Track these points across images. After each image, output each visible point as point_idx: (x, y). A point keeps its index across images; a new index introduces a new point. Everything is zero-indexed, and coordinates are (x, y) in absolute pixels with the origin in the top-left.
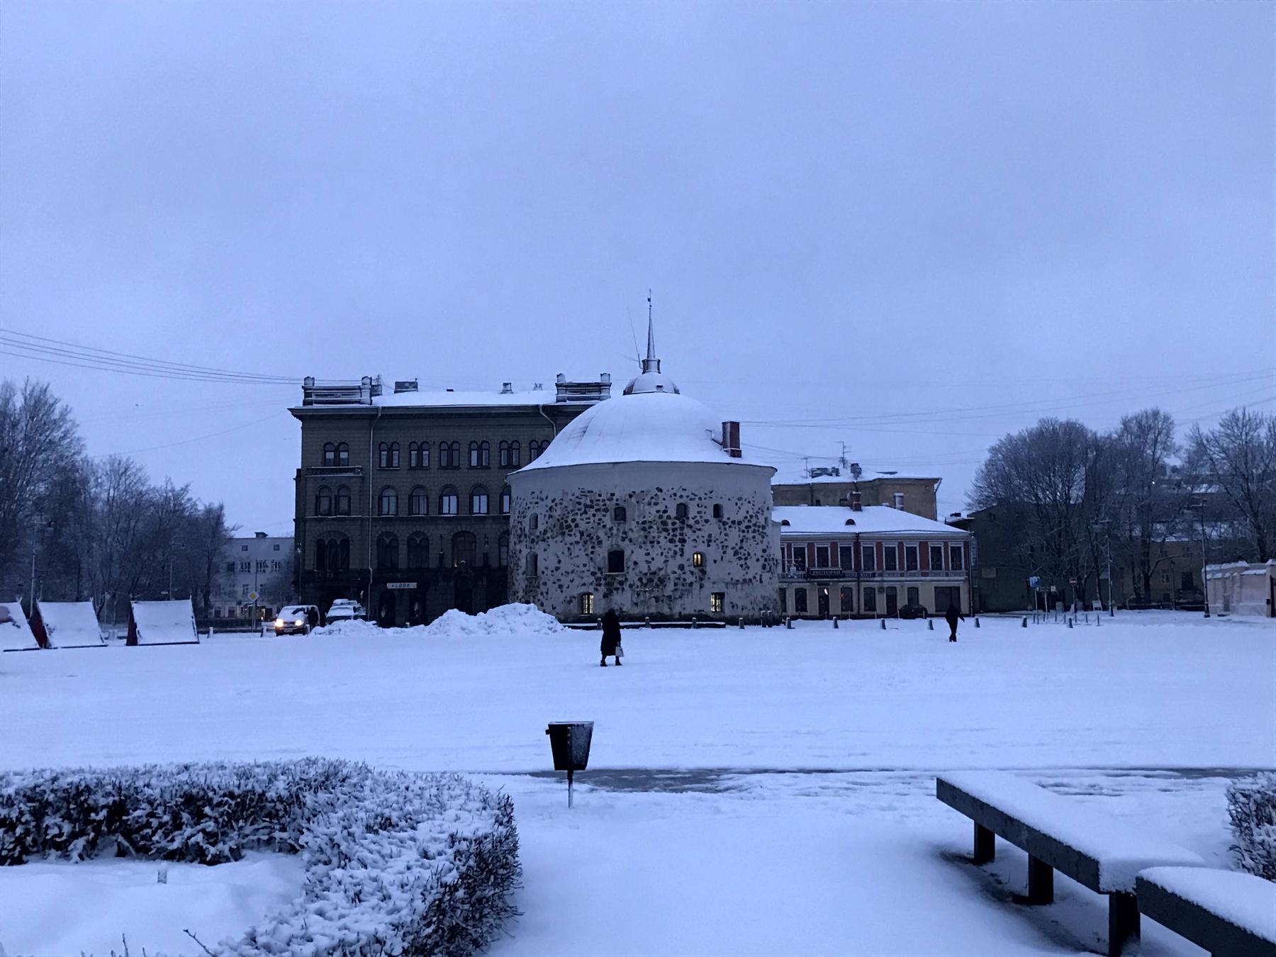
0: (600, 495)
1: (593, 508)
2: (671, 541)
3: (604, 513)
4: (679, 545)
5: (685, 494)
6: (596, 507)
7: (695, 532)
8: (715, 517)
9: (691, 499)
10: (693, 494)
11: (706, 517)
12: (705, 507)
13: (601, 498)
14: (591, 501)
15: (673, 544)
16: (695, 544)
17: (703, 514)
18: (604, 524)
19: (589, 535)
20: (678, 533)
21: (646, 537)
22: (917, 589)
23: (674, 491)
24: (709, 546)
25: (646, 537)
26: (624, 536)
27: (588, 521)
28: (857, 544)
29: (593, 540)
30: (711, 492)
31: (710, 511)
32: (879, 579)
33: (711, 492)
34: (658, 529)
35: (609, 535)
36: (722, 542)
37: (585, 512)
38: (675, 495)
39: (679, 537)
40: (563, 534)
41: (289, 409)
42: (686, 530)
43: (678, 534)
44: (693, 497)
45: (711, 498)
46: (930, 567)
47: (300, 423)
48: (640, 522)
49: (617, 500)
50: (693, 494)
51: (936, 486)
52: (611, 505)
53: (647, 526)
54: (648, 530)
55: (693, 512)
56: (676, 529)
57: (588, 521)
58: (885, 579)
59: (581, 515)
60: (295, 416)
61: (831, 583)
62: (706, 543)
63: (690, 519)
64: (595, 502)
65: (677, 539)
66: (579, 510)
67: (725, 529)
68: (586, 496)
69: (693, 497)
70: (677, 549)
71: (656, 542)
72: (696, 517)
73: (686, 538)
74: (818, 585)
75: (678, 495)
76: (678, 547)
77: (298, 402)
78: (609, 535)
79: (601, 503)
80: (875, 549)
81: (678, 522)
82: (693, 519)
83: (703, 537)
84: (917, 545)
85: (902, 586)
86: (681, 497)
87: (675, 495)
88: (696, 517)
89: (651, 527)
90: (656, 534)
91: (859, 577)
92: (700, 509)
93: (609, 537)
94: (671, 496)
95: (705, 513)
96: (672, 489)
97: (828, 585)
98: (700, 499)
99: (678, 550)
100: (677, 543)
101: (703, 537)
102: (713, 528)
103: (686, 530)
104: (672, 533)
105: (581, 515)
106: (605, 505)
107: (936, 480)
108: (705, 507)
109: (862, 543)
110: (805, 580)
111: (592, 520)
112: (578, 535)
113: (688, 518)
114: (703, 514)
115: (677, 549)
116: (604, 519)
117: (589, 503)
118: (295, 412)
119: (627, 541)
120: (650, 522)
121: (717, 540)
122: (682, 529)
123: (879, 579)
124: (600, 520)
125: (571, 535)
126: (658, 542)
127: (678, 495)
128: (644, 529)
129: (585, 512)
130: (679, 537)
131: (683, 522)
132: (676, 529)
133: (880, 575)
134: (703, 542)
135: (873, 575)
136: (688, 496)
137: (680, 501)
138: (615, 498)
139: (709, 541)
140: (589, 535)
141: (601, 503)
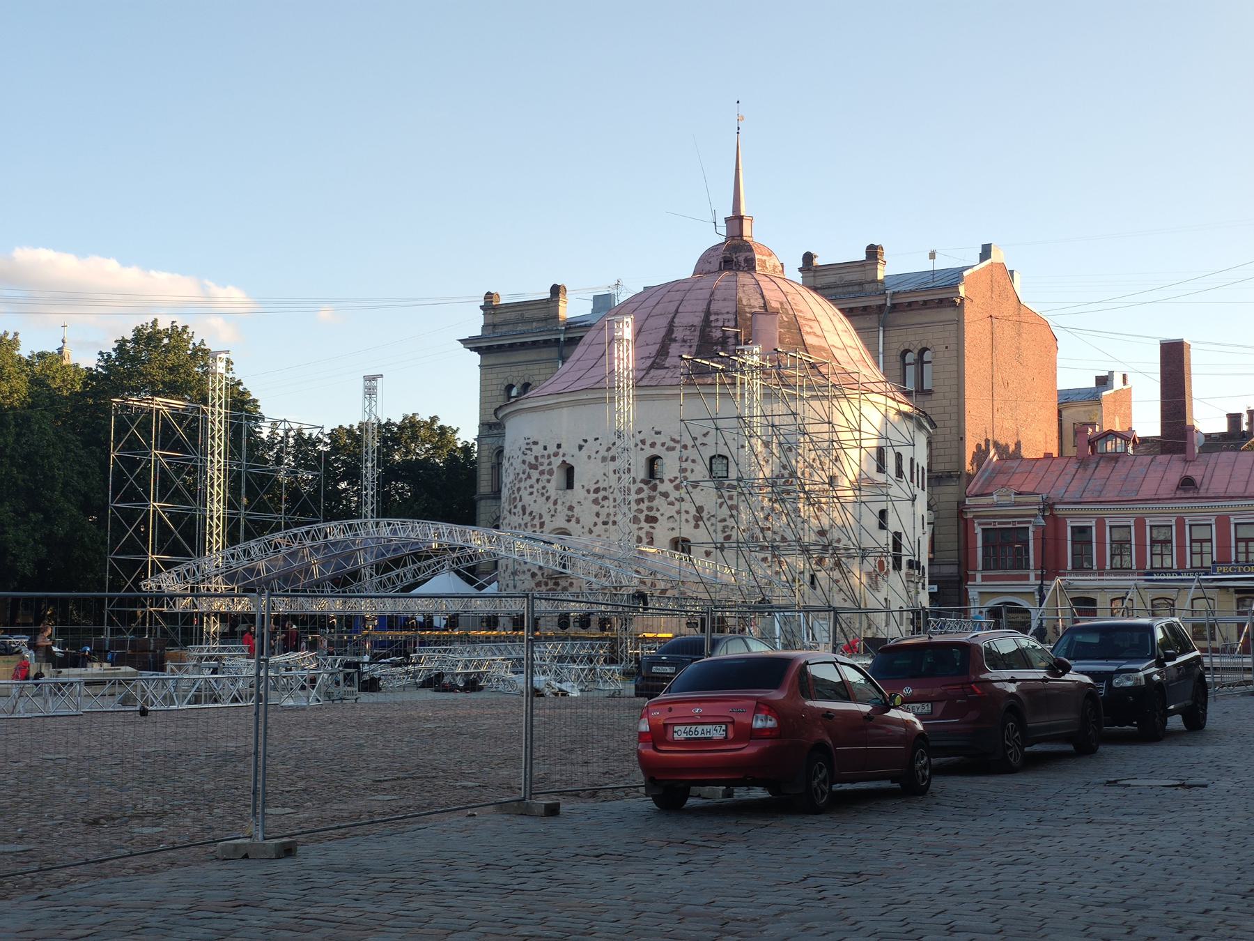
0: (545, 448)
1: (537, 469)
2: (636, 520)
3: (549, 477)
4: (646, 526)
5: (659, 440)
6: (541, 468)
7: (672, 504)
8: (835, 477)
9: (669, 449)
10: (673, 440)
11: (692, 478)
12: (693, 461)
13: (546, 453)
14: (536, 458)
15: (636, 526)
16: (671, 525)
17: (688, 474)
18: (548, 494)
19: (531, 513)
20: (643, 506)
21: (598, 515)
23: (641, 437)
24: (697, 526)
25: (598, 515)
26: (570, 513)
27: (531, 490)
29: (534, 522)
30: (705, 435)
31: (700, 471)
33: (705, 435)
34: (615, 500)
35: (552, 513)
36: (725, 520)
37: (529, 477)
38: (643, 442)
39: (646, 512)
40: (510, 512)
41: (464, 342)
42: (659, 502)
43: (645, 509)
44: (672, 444)
45: (704, 444)
47: (476, 357)
48: (592, 491)
49: (564, 455)
50: (673, 440)
52: (557, 462)
53: (602, 494)
54: (603, 503)
55: (670, 467)
56: (642, 500)
57: (531, 490)
59: (526, 479)
60: (471, 349)
62: (693, 523)
63: (666, 482)
64: (540, 460)
65: (642, 517)
66: (524, 473)
67: (731, 498)
68: (531, 450)
69: (672, 444)
70: (642, 534)
71: (610, 523)
72: (676, 478)
73: (658, 515)
75: (648, 443)
76: (644, 531)
77: (474, 325)
78: (552, 513)
79: (546, 461)
81: (645, 487)
82: (671, 481)
83: (687, 512)
86: (653, 445)
87: (643, 442)
88: (676, 478)
89: (605, 498)
90: (612, 511)
92: (684, 465)
93: (553, 516)
94: (636, 445)
95: (692, 471)
96: (640, 432)
98: (685, 447)
99: (643, 536)
100: (643, 524)
101: (687, 512)
102: (707, 497)
103: (659, 502)
104: (634, 506)
105: (526, 479)
106: (549, 464)
108: (693, 461)
111: (535, 490)
112: (521, 512)
113: (662, 481)
114: (688, 474)
115: (642, 534)
116: (548, 486)
117: (533, 462)
118: (469, 343)
119: (574, 520)
120: (605, 489)
121: (713, 516)
122: (651, 499)
124: (544, 488)
125: (515, 514)
126: (614, 523)
127: (648, 443)
128: (596, 502)
129: (529, 477)
130: (646, 512)
131: (654, 488)
132: (642, 500)
134: (687, 521)
136: (663, 444)
137: (650, 452)
138: (561, 451)
139: (698, 519)
140: (531, 513)
141: (546, 461)
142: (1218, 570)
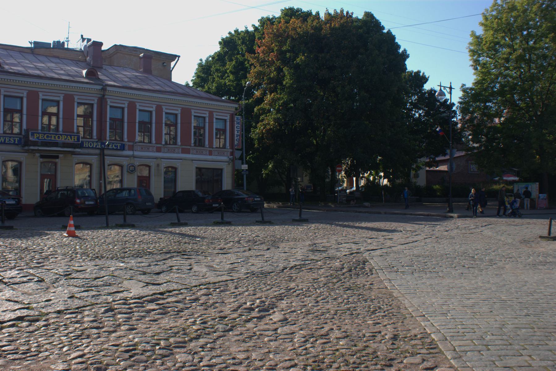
22: (175, 169)
28: (102, 101)
32: (130, 153)
46: (193, 142)
51: (173, 64)
58: (136, 153)
61: (61, 156)
74: (42, 157)
80: (126, 110)
84: (179, 112)
85: (158, 165)
91: (102, 150)
97: (57, 157)
107: (173, 57)
109: (109, 101)
110: (18, 148)
123: (130, 153)
133: (131, 148)
135: (123, 148)
142: (35, 137)
